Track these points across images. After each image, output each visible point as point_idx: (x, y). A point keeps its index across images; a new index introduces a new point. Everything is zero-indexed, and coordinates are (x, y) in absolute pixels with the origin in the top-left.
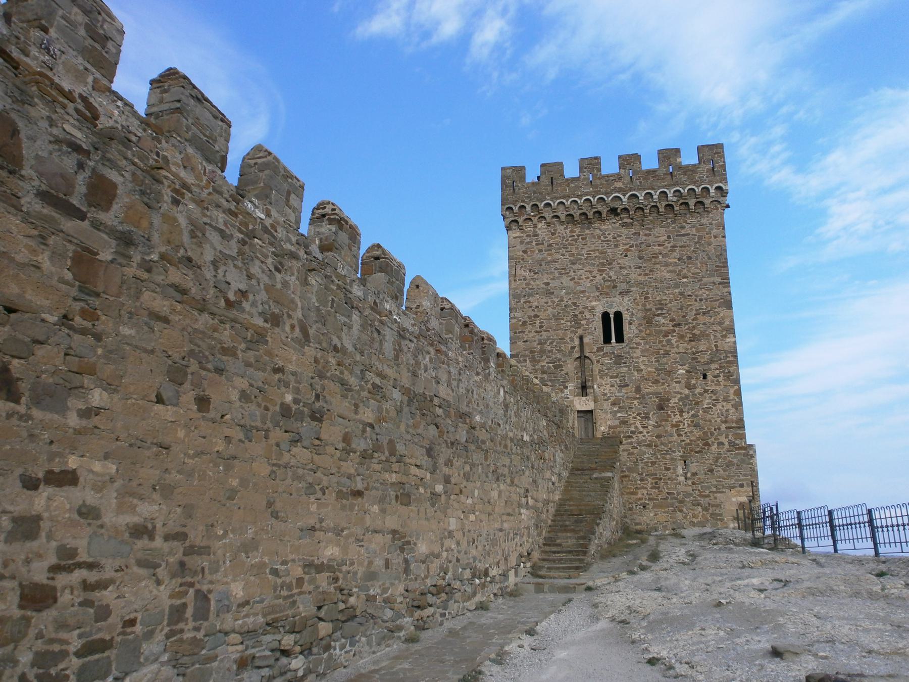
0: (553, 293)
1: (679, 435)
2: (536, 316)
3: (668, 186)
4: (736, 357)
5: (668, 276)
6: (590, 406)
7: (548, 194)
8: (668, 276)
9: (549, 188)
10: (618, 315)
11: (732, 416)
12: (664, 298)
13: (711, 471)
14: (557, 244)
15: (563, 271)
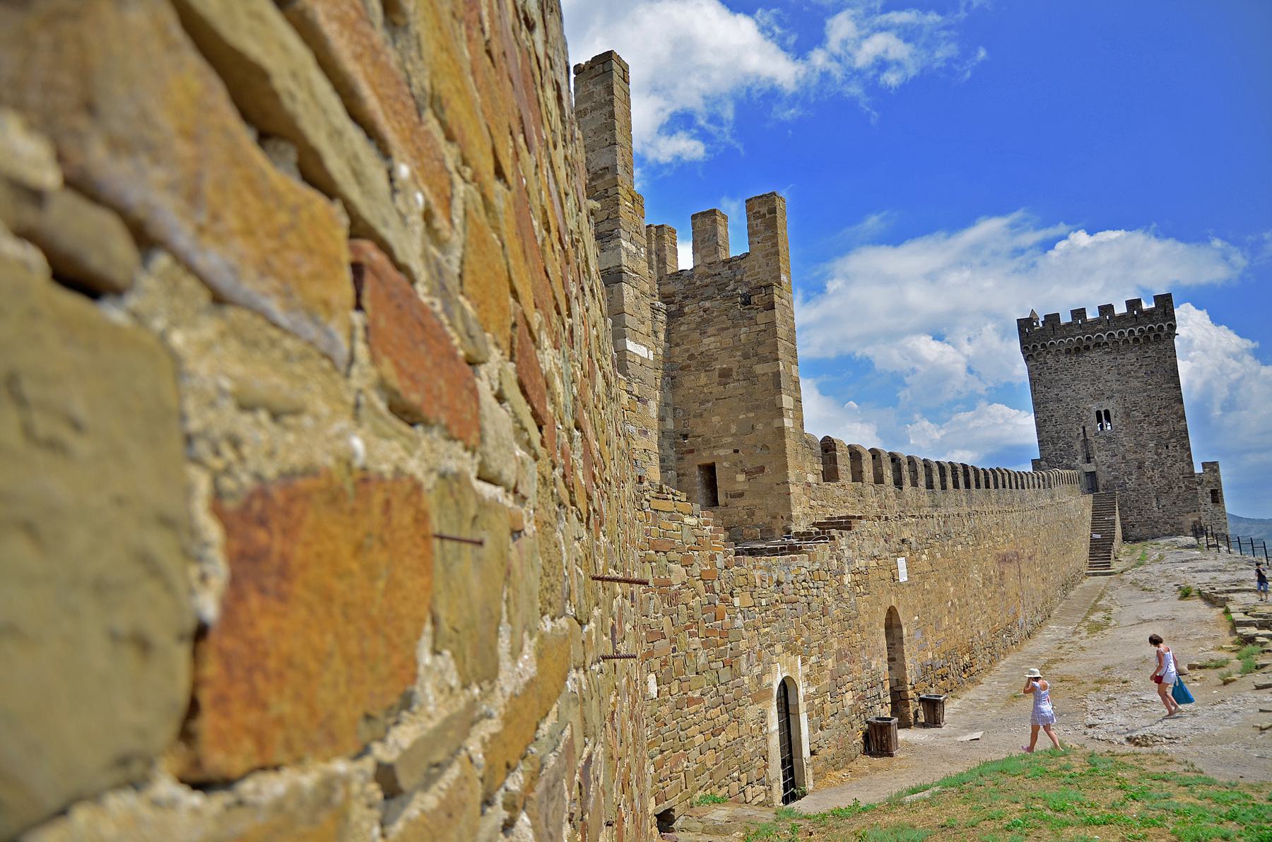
0: (1062, 400)
1: (1152, 484)
2: (1052, 416)
3: (1134, 326)
4: (1187, 434)
5: (1138, 385)
6: (1093, 469)
7: (1052, 336)
8: (1138, 385)
9: (1052, 332)
10: (1107, 412)
11: (1187, 470)
12: (1137, 399)
13: (1175, 503)
14: (1061, 368)
15: (1067, 386)
